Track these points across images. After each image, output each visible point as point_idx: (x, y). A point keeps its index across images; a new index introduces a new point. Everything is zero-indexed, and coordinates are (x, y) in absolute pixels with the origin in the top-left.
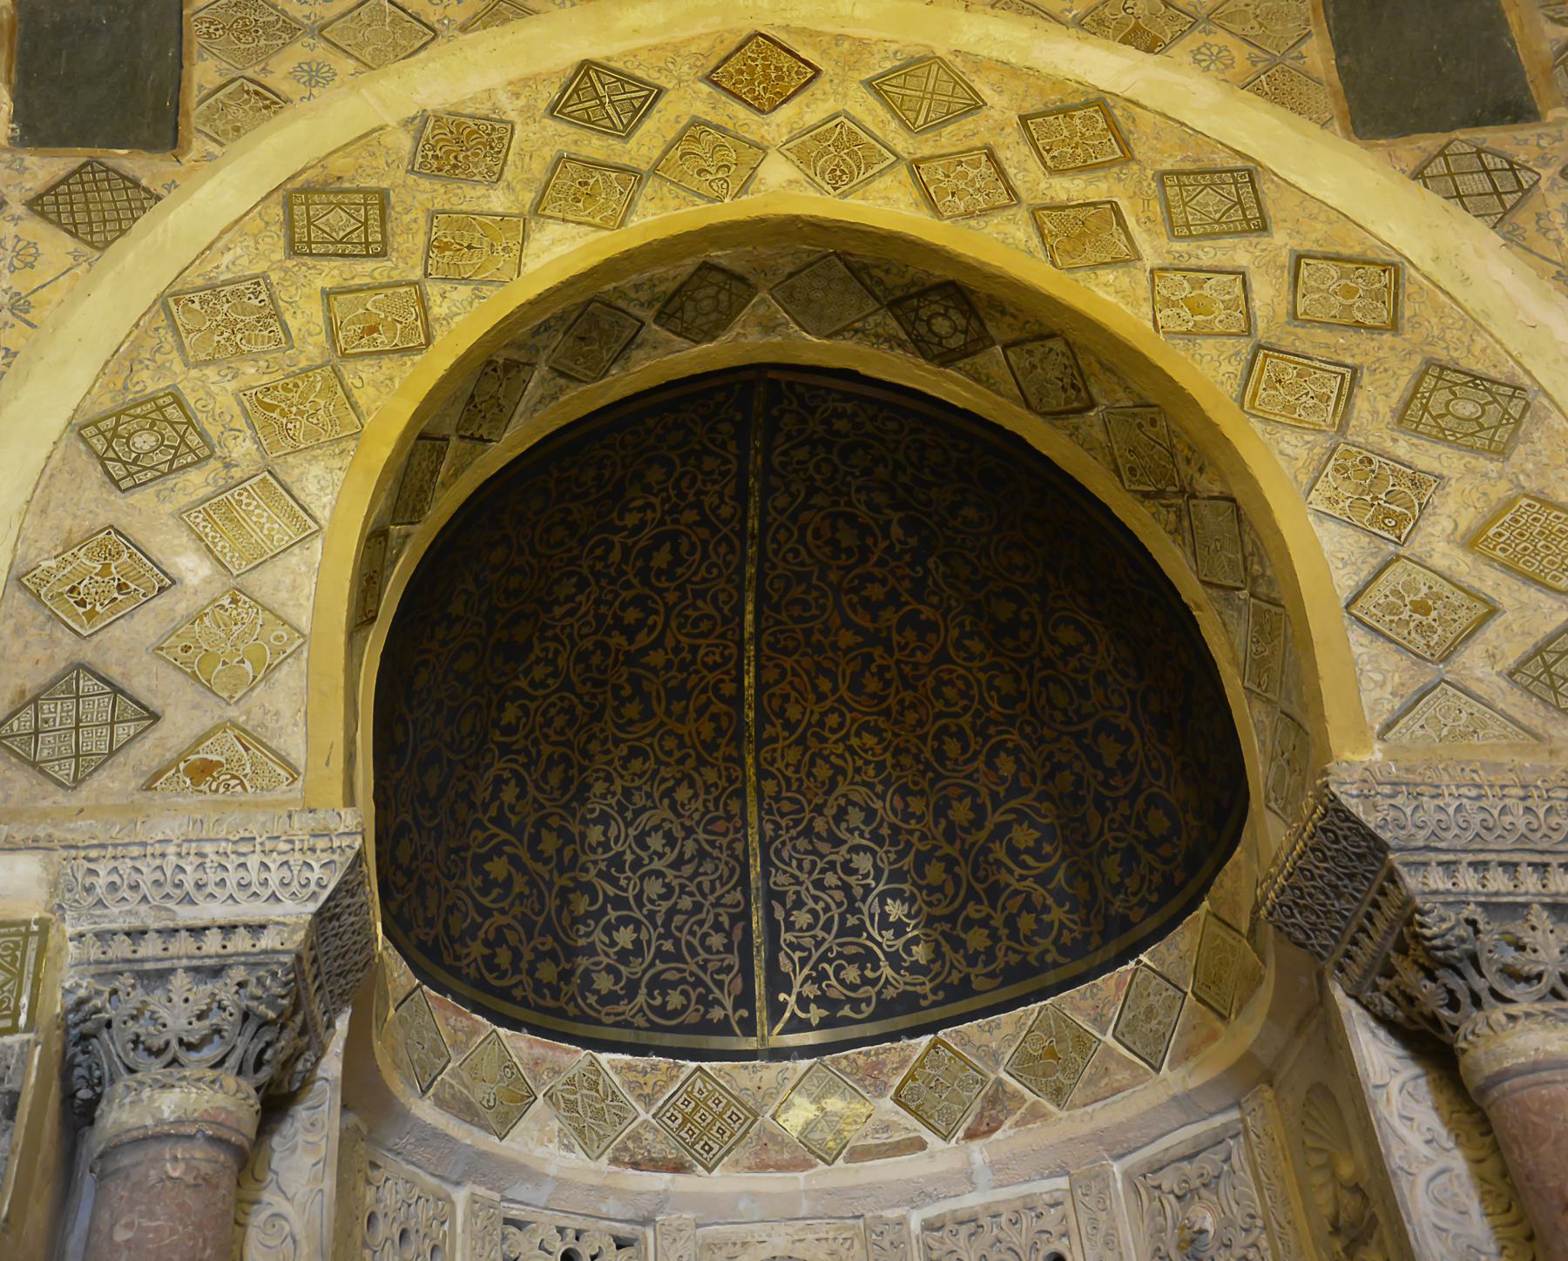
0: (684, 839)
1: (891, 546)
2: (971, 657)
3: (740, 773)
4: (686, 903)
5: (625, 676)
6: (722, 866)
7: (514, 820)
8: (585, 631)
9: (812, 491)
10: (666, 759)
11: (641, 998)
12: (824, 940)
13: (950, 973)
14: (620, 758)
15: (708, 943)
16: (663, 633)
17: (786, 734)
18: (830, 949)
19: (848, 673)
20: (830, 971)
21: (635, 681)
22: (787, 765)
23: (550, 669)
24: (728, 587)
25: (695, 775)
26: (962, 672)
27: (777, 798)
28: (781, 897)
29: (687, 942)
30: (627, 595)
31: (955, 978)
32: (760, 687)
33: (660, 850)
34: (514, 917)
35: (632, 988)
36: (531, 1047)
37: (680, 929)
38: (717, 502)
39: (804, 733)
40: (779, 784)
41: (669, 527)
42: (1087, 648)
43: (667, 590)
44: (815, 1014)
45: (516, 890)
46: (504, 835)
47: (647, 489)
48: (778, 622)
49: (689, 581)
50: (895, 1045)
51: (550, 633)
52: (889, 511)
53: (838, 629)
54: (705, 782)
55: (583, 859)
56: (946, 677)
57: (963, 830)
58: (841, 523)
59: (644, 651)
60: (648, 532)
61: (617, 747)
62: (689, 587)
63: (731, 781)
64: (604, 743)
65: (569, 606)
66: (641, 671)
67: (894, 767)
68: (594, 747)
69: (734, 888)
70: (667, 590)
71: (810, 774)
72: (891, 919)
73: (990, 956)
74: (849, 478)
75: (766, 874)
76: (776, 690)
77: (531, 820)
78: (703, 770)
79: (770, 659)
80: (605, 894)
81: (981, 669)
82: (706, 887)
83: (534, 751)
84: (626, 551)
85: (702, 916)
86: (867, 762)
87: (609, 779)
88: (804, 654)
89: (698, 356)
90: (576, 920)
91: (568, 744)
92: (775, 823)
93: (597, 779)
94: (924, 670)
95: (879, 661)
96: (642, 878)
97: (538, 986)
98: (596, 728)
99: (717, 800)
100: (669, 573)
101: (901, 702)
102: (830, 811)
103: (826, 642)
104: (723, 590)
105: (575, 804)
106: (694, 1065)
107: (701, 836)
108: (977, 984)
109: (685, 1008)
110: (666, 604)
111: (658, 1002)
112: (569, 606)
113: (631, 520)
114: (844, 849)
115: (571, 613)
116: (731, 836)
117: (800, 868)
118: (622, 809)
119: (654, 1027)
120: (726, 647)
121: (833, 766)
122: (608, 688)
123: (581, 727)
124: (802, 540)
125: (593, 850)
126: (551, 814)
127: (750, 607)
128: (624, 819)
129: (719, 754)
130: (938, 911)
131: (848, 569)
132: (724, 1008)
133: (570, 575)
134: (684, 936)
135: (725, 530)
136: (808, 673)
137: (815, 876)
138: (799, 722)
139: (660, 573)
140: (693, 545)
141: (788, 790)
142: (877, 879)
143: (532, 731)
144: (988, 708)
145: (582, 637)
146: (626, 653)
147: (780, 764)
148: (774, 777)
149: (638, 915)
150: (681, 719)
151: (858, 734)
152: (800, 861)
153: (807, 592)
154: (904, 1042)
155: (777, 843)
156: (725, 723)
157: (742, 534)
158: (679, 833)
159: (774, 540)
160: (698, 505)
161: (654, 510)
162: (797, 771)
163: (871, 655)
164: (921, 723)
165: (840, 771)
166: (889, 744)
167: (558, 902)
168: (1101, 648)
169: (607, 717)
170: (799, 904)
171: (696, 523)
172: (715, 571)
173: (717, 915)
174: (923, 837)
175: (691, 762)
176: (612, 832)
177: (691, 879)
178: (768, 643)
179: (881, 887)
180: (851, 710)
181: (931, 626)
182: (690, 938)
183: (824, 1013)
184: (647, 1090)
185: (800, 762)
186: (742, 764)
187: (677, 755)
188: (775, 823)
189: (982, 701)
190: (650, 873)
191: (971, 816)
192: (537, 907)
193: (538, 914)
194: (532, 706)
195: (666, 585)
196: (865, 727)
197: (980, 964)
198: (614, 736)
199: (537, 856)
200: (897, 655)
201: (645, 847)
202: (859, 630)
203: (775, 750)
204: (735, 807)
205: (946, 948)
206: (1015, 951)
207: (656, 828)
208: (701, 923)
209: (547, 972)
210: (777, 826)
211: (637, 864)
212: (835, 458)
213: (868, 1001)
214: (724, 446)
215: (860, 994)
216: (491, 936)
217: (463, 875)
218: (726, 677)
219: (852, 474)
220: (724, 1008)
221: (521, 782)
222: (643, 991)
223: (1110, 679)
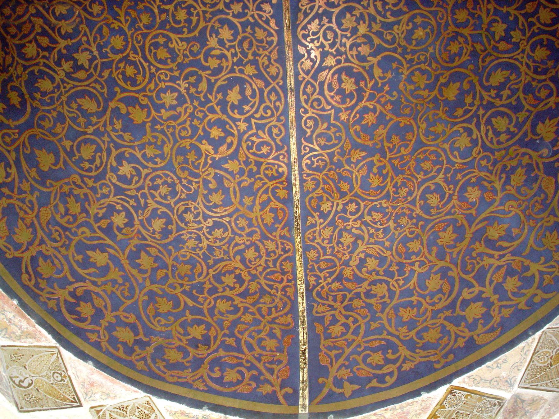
0: (249, 281)
1: (376, 83)
2: (437, 136)
3: (291, 248)
5: (212, 175)
8: (184, 134)
9: (324, 55)
12: (353, 341)
13: (456, 341)
15: (263, 344)
16: (237, 150)
17: (322, 221)
18: (359, 346)
19: (359, 177)
20: (360, 359)
21: (219, 179)
22: (323, 240)
23: (159, 152)
24: (278, 124)
26: (433, 148)
27: (318, 260)
28: (320, 320)
29: (246, 342)
30: (211, 117)
31: (461, 342)
32: (304, 194)
33: (231, 285)
35: (198, 363)
37: (241, 333)
38: (267, 63)
39: (333, 221)
40: (318, 253)
41: (238, 75)
42: (513, 77)
43: (239, 120)
44: (348, 388)
47: (221, 42)
48: (312, 150)
49: (252, 116)
50: (417, 399)
51: (159, 127)
52: (369, 58)
53: (350, 151)
54: (267, 250)
56: (422, 156)
57: (449, 247)
58: (344, 77)
59: (225, 160)
60: (223, 77)
61: (205, 220)
62: (253, 121)
63: (284, 250)
64: (197, 215)
65: (173, 113)
66: (222, 173)
67: (395, 229)
68: (189, 217)
69: (286, 314)
70: (239, 120)
71: (339, 243)
72: (405, 319)
73: (487, 317)
74: (344, 40)
75: (310, 308)
76: (314, 195)
77: (135, 242)
78: (265, 242)
79: (308, 175)
81: (443, 142)
82: (265, 311)
83: (142, 201)
84: (211, 86)
86: (377, 230)
88: (329, 170)
91: (168, 206)
92: (315, 276)
93: (190, 238)
94: (407, 158)
95: (378, 164)
96: (216, 299)
98: (192, 204)
99: (275, 261)
100: (239, 107)
101: (395, 186)
102: (353, 263)
103: (343, 160)
104: (275, 126)
107: (263, 281)
108: (479, 341)
109: (239, 382)
110: (239, 131)
111: (217, 375)
112: (173, 113)
113: (213, 63)
114: (365, 284)
115: (175, 118)
116: (285, 283)
117: (335, 300)
119: (210, 390)
120: (280, 166)
121: (354, 235)
122: (201, 180)
123: (180, 200)
124: (321, 93)
125: (182, 278)
126: (152, 246)
127: (293, 140)
128: (207, 265)
129: (277, 234)
130: (440, 306)
131: (352, 108)
133: (173, 90)
134: (245, 337)
135: (274, 84)
136: (332, 180)
137: (345, 303)
138: (330, 212)
139: (233, 107)
140: (253, 90)
141: (325, 254)
142: (391, 297)
143: (142, 187)
144: (453, 164)
145: (182, 138)
146: (213, 159)
147: (318, 240)
148: (314, 248)
149: (210, 320)
150: (250, 208)
151: (369, 214)
152: (335, 297)
153: (328, 128)
154: (425, 395)
155: (318, 288)
156: (280, 215)
157: (284, 88)
158: (247, 278)
159: (305, 93)
160: (254, 63)
161: (227, 60)
162: (330, 242)
163: (372, 161)
164: (410, 193)
165: (358, 237)
166: (391, 215)
168: (523, 69)
169: (199, 199)
170: (334, 321)
171: (254, 75)
172: (269, 112)
174: (422, 264)
175: (257, 237)
176: (198, 270)
177: (253, 305)
178: (306, 164)
179: (395, 302)
180: (363, 200)
181: (408, 128)
182: (249, 339)
183: (356, 387)
185: (331, 236)
186: (291, 240)
187: (247, 230)
188: (315, 276)
189: (449, 161)
190: (222, 297)
191: (454, 236)
193: (128, 298)
194: (144, 172)
195: (237, 116)
196: (374, 209)
197: (480, 326)
198: (203, 212)
200: (388, 156)
201: (222, 282)
202: (364, 148)
203: (314, 232)
204: (287, 266)
205: (450, 327)
206: (506, 307)
207: (230, 272)
210: (318, 278)
212: (334, 26)
213: (391, 374)
214: (267, 22)
215: (385, 370)
218: (281, 186)
219: (346, 36)
220: (272, 385)
221: (129, 215)
222: (206, 365)
223: (534, 84)
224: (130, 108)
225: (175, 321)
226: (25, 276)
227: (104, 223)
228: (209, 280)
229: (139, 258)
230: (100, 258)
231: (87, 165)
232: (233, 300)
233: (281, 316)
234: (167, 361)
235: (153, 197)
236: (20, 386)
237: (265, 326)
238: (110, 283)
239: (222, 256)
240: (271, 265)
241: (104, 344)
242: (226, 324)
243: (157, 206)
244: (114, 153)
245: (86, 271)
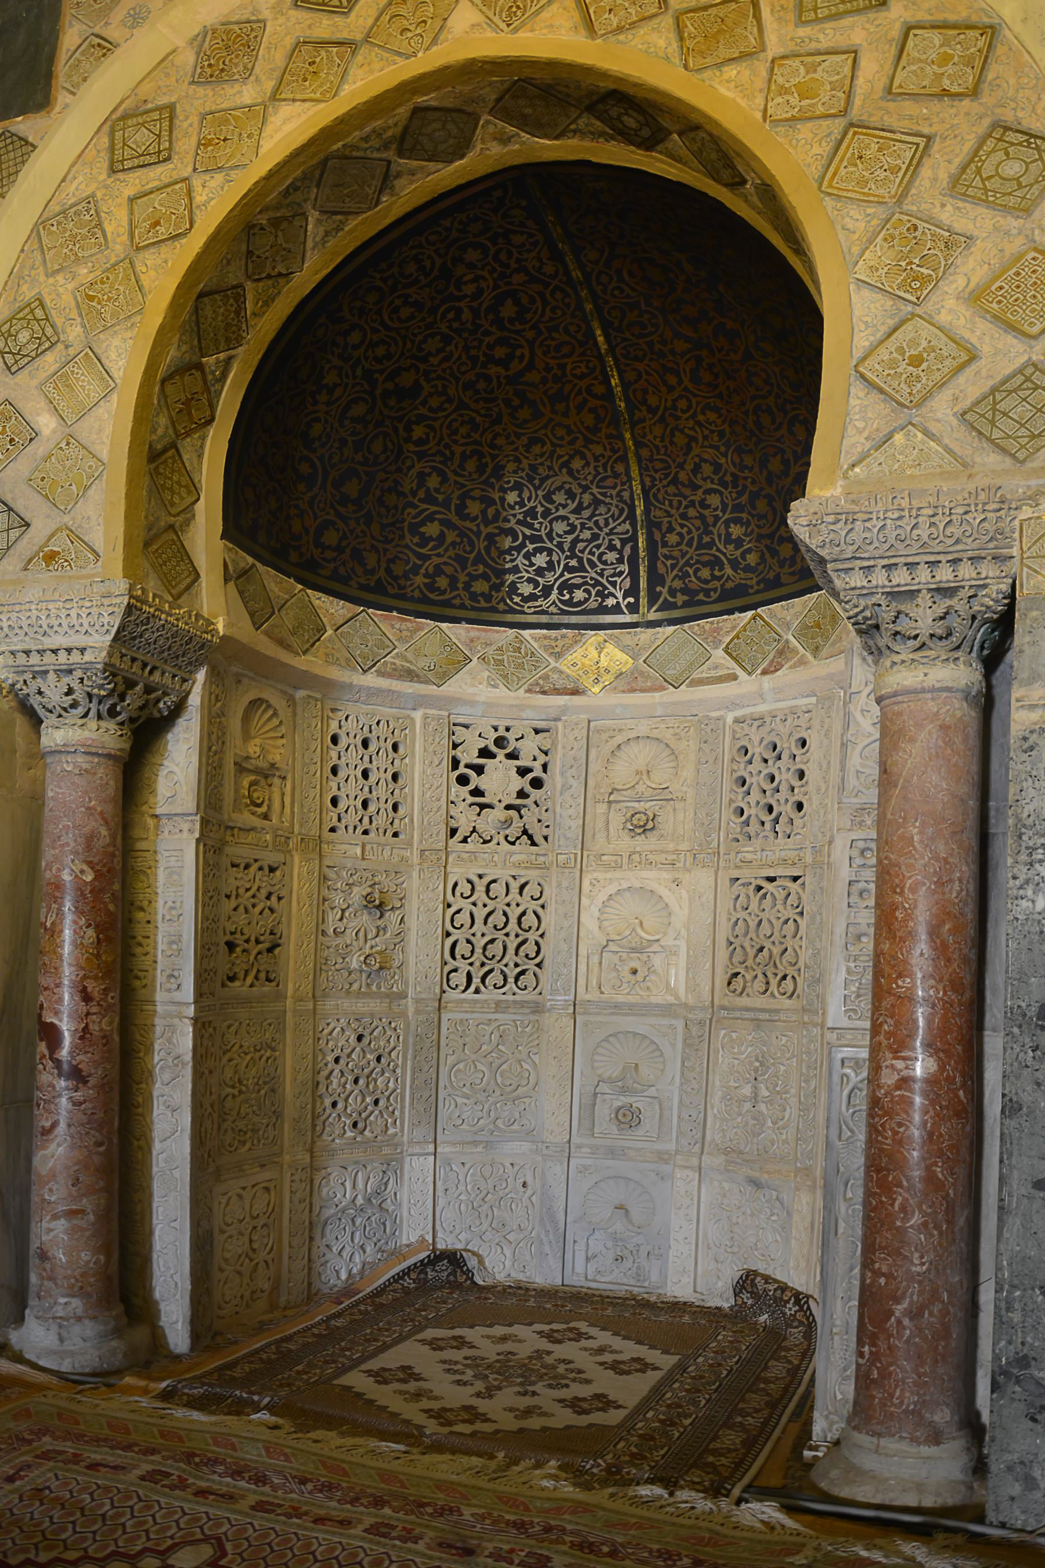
6: (613, 508)
7: (440, 497)
34: (450, 557)
46: (433, 508)
80: (523, 533)
89: (456, 171)
96: (551, 522)
97: (474, 597)
107: (595, 490)
149: (549, 545)
184: (557, 650)
190: (557, 519)
192: (468, 549)
209: (480, 587)
216: (431, 570)
217: (402, 537)
232: (568, 519)
234: (521, 595)
240: (600, 470)
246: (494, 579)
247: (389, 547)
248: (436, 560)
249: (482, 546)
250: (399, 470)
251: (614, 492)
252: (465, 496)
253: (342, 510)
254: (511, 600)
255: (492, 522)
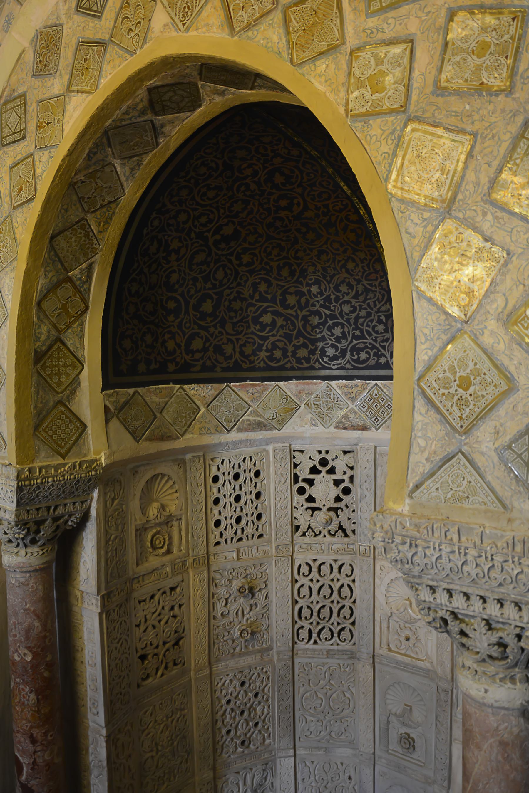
0: (357, 285)
4: (363, 313)
10: (334, 251)
11: (348, 357)
14: (315, 256)
15: (376, 329)
25: (353, 256)
29: (366, 330)
35: (343, 353)
36: (297, 386)
45: (279, 324)
55: (311, 301)
68: (300, 254)
82: (372, 305)
83: (268, 267)
85: (372, 318)
87: (314, 265)
90: (313, 328)
93: (309, 266)
96: (341, 305)
105: (301, 279)
106: (374, 382)
107: (365, 282)
109: (368, 359)
111: (356, 357)
116: (379, 280)
118: (324, 277)
119: (355, 368)
125: (316, 296)
128: (327, 281)
132: (386, 357)
134: (364, 328)
149: (342, 321)
158: (354, 283)
167: (303, 322)
173: (379, 316)
176: (323, 287)
177: (364, 302)
182: (367, 328)
194: (257, 251)
199: (287, 307)
201: (340, 291)
207: (343, 282)
208: (372, 321)
211: (337, 299)
220: (386, 357)
222: (349, 353)
224: (221, 233)
225: (324, 328)
226: (244, 366)
227: (257, 296)
228: (332, 292)
229: (287, 300)
230: (267, 319)
231: (226, 280)
232: (351, 302)
233: (383, 305)
234: (328, 356)
235: (272, 260)
236: (274, 419)
237: (374, 315)
238: (281, 330)
239: (333, 272)
241: (295, 365)
242: (352, 321)
243: (277, 263)
244: (233, 258)
245: (266, 332)
246: (311, 347)
247: (240, 336)
248: (272, 339)
249: (300, 325)
250: (239, 284)
251: (377, 283)
252: (285, 293)
253: (202, 323)
254: (323, 360)
255: (305, 307)
